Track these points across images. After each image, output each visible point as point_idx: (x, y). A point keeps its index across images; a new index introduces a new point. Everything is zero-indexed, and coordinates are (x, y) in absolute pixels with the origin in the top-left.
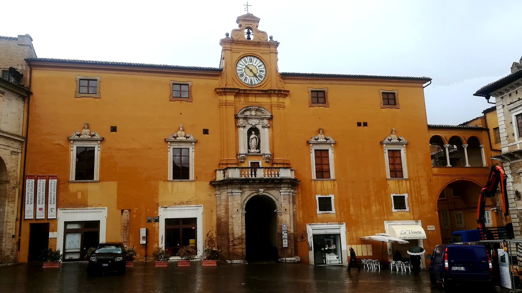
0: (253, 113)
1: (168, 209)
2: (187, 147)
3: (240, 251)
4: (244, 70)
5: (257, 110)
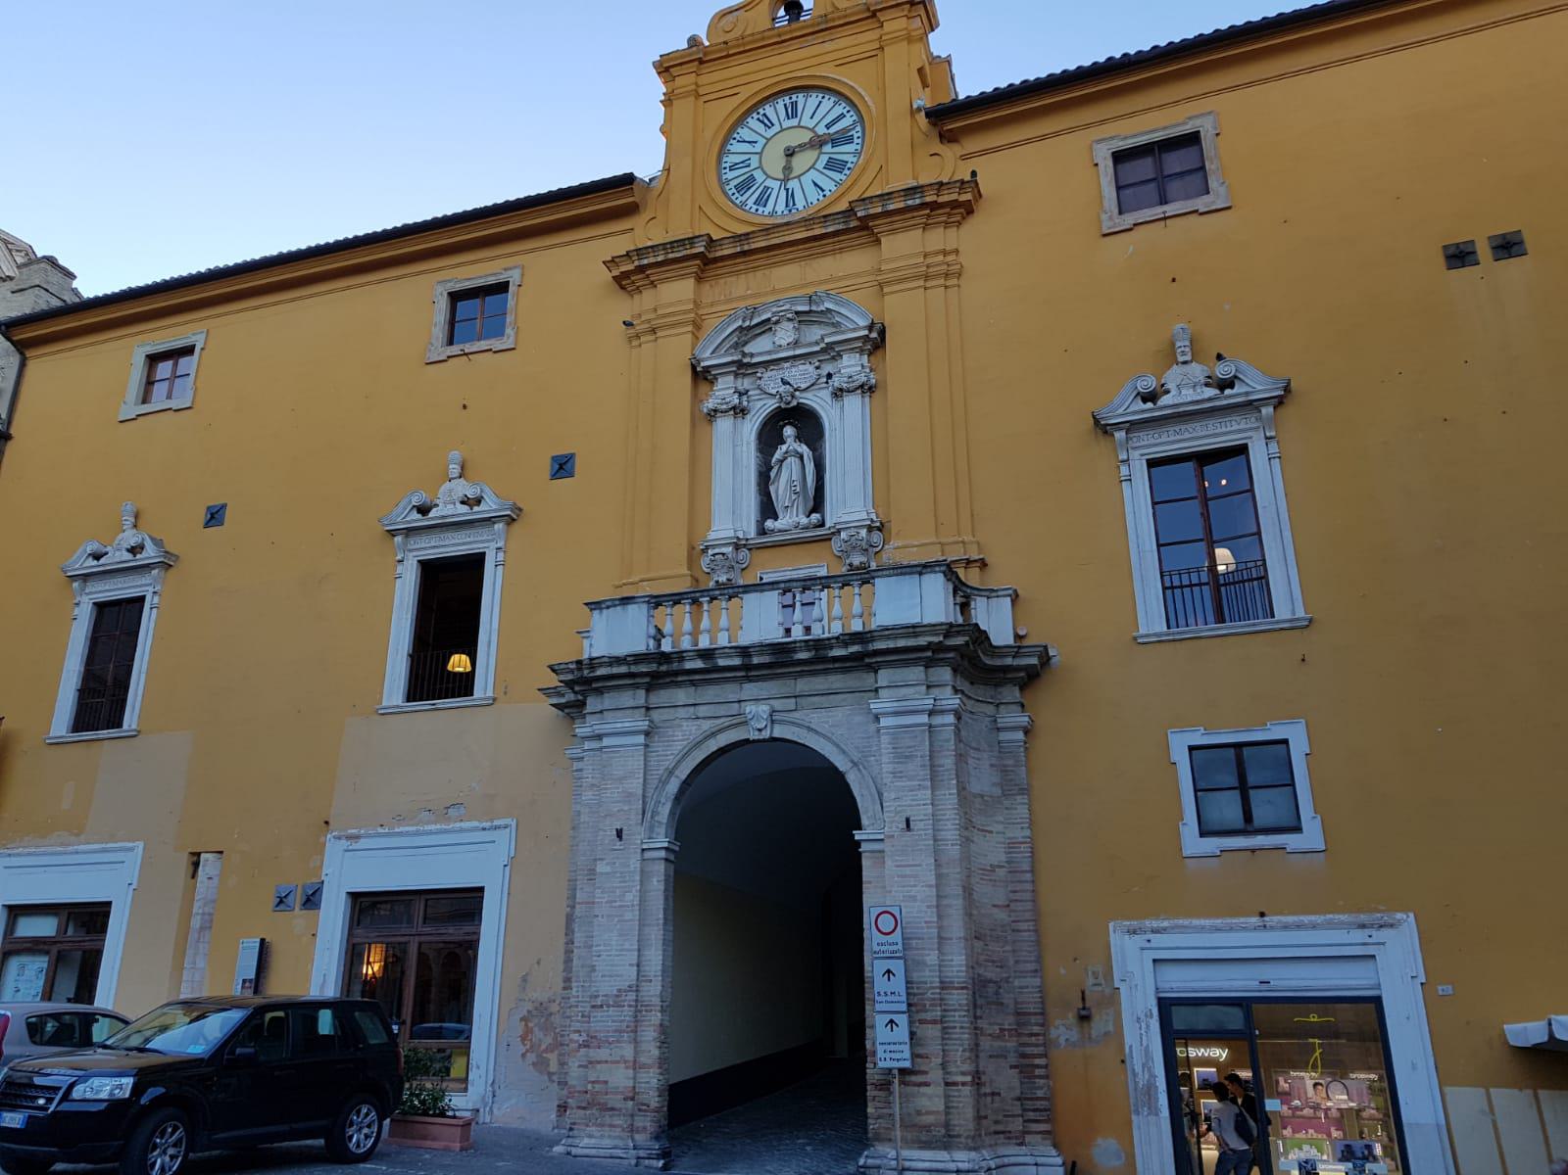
0: (785, 334)
1: (363, 843)
2: (475, 548)
3: (620, 1078)
4: (806, 180)
5: (803, 319)
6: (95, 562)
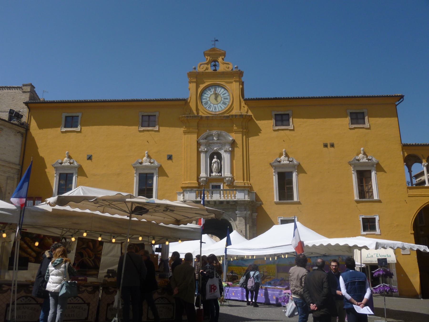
6: (60, 165)
